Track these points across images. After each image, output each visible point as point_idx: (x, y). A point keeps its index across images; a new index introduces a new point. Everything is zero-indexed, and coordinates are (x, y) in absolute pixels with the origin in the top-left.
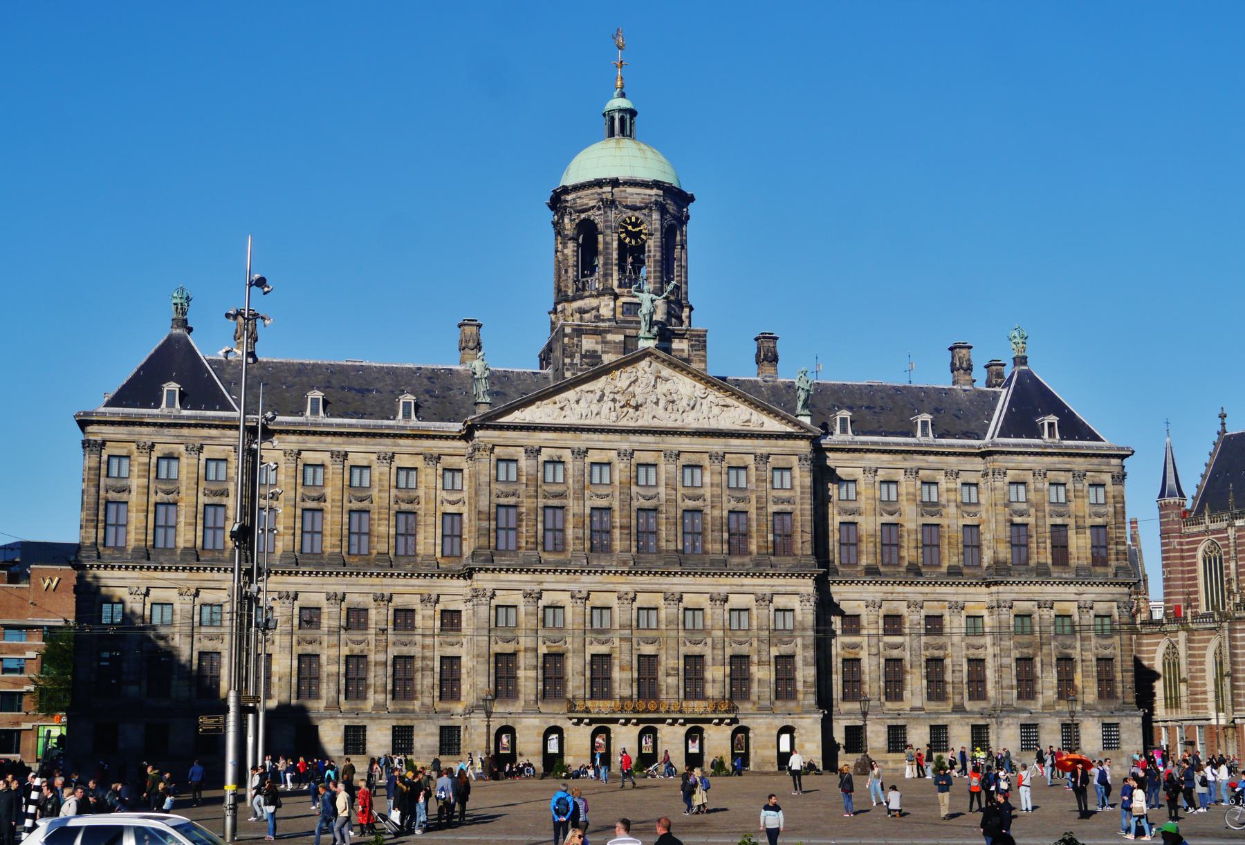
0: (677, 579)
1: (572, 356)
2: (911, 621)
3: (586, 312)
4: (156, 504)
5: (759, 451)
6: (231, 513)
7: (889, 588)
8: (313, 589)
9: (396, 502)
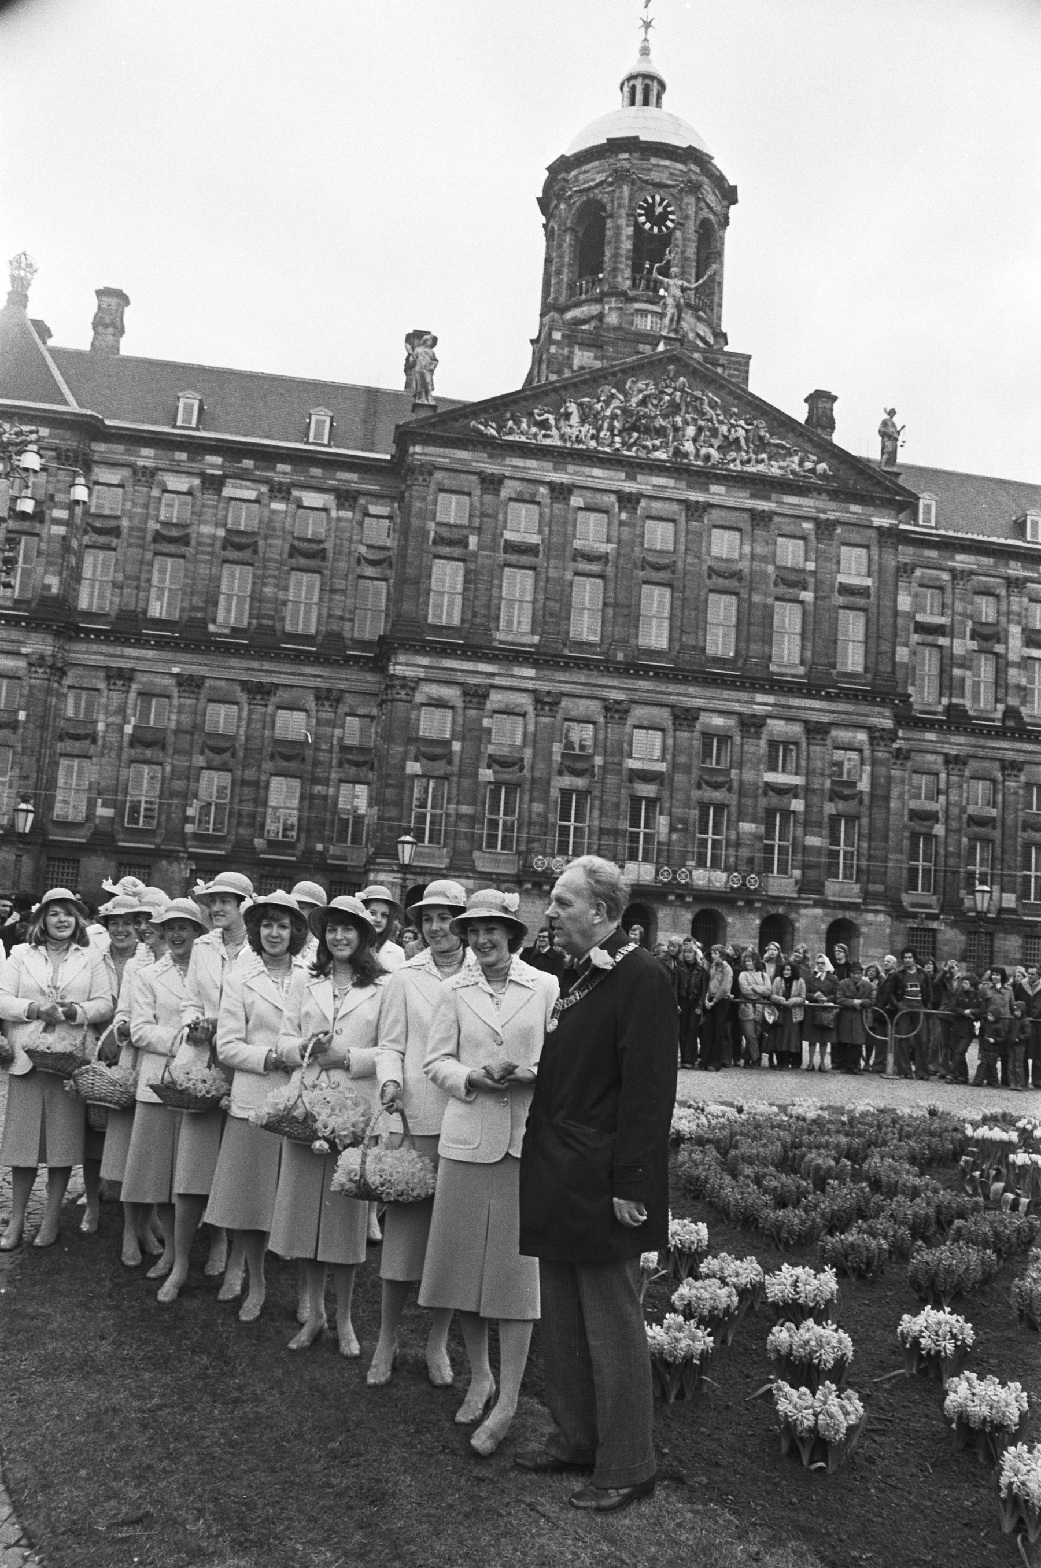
0: (691, 690)
1: (559, 373)
2: (1009, 788)
3: (584, 322)
5: (822, 516)
7: (982, 742)
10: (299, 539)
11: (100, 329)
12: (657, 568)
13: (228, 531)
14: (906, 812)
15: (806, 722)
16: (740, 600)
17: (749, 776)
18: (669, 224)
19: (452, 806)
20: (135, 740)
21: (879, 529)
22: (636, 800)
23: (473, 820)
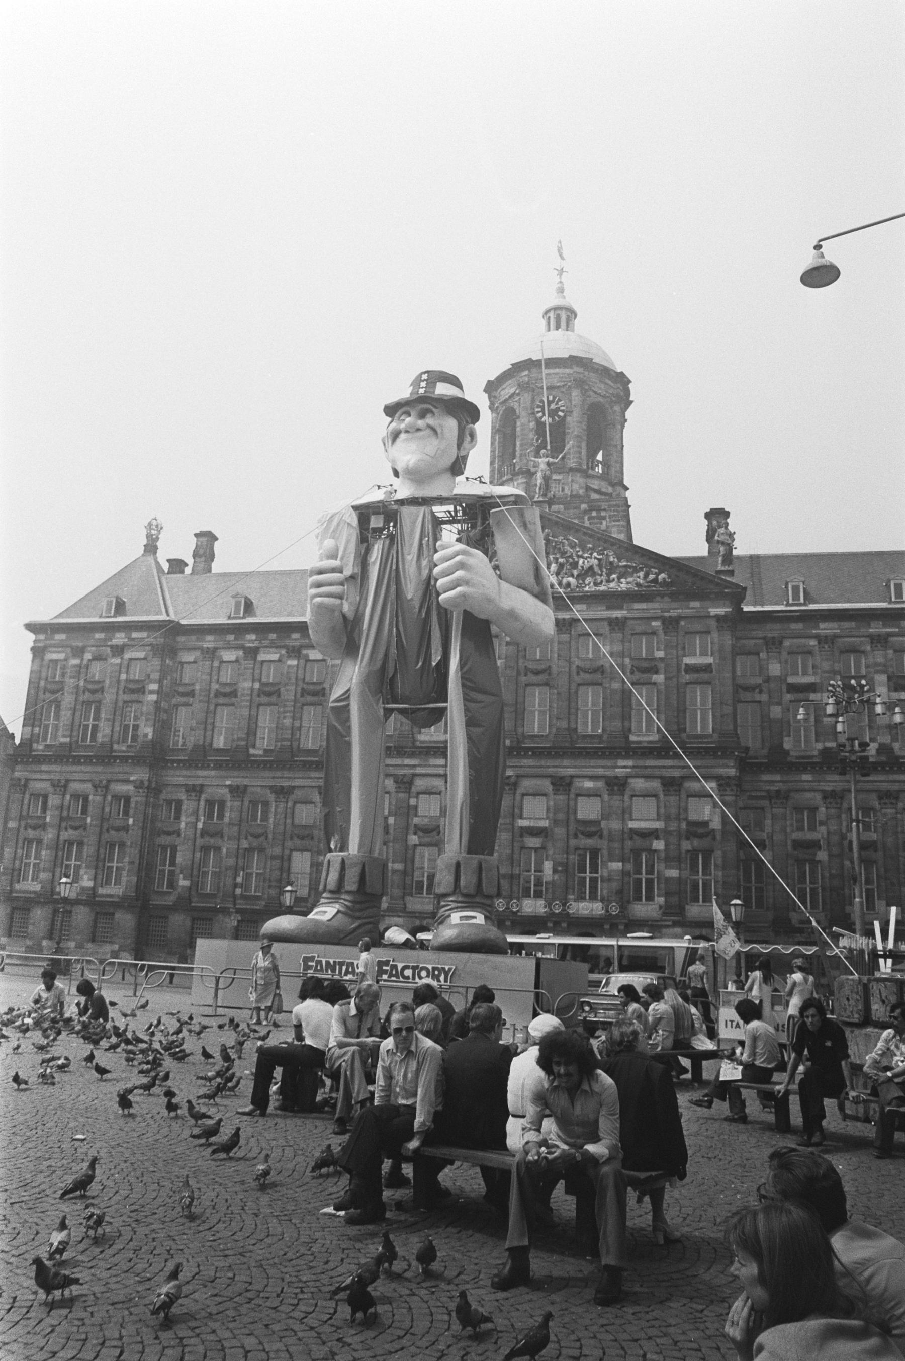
0: (566, 762)
4: (84, 702)
5: (666, 614)
6: (145, 708)
8: (217, 782)
9: (302, 695)
10: (308, 683)
11: (198, 560)
12: (537, 673)
13: (263, 684)
14: (789, 843)
15: (661, 777)
16: (605, 688)
17: (615, 825)
18: (561, 414)
20: (204, 833)
21: (718, 618)
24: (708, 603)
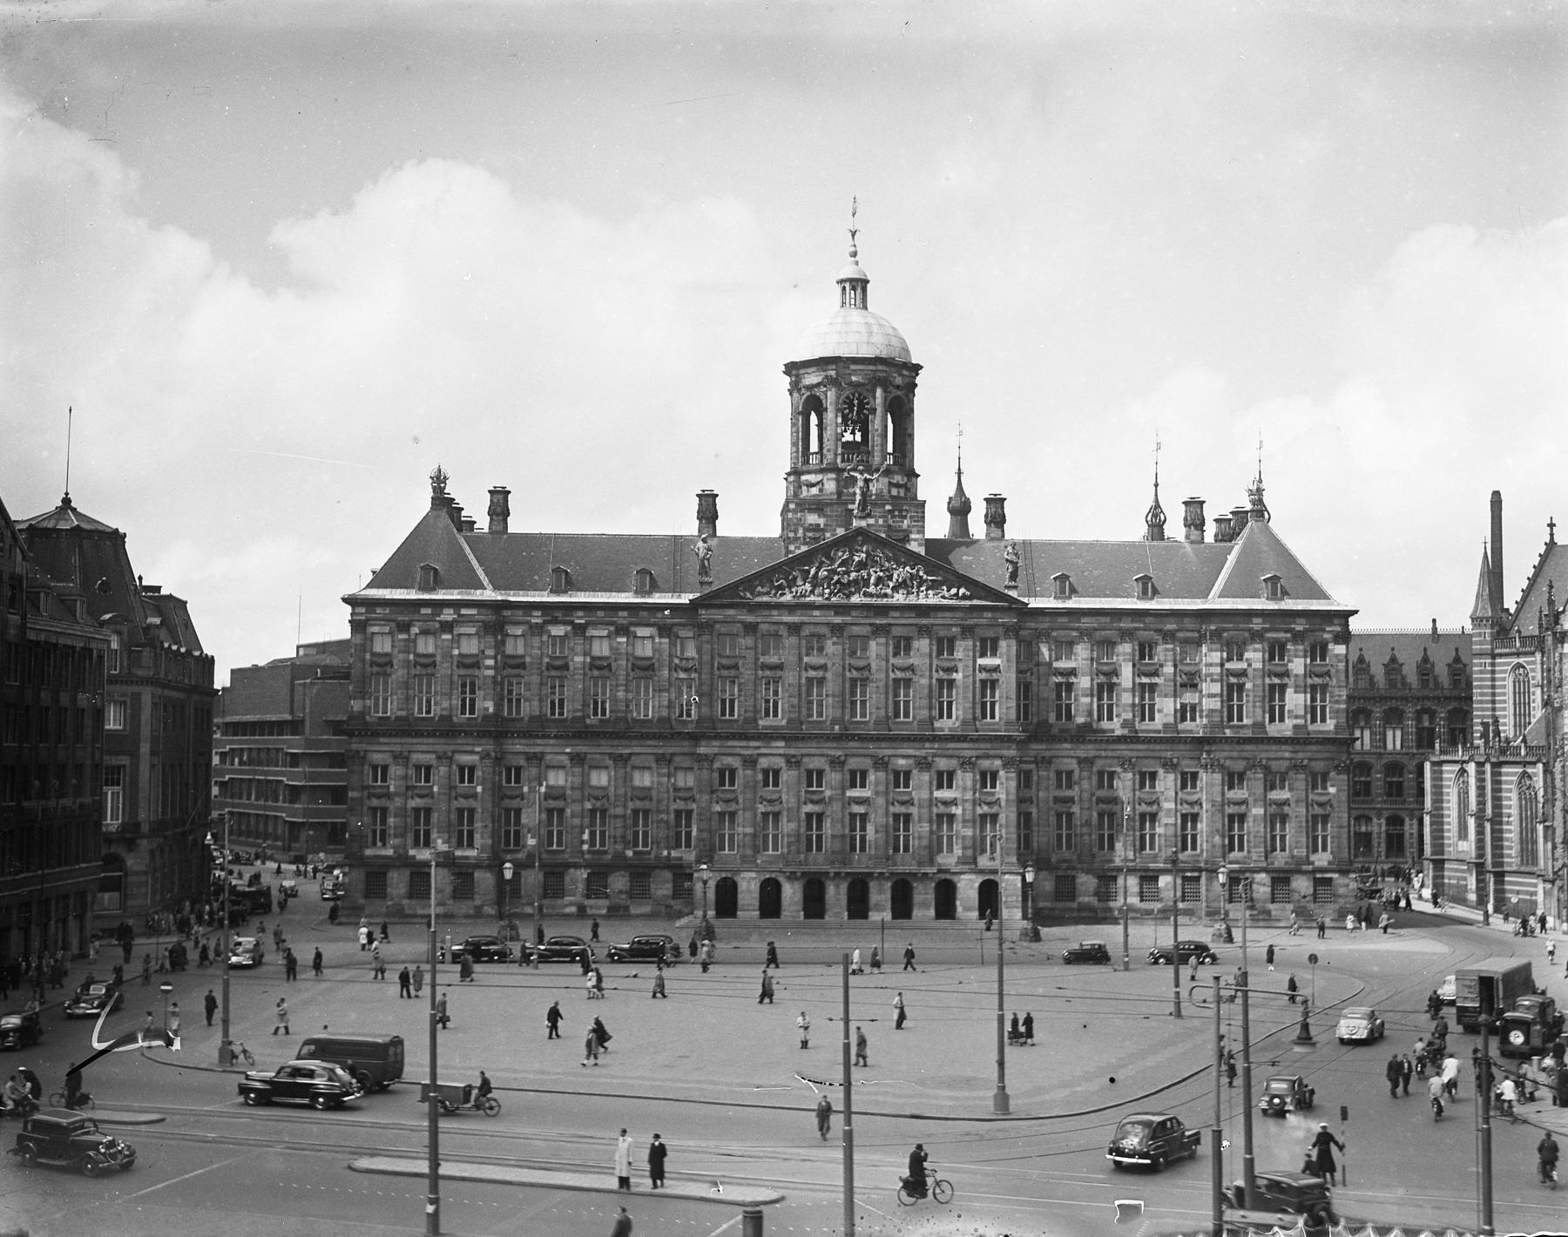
0: (883, 745)
1: (795, 532)
3: (813, 485)
13: (593, 658)
17: (925, 795)
19: (740, 829)
20: (547, 796)
22: (853, 816)
23: (754, 836)
24: (998, 614)
